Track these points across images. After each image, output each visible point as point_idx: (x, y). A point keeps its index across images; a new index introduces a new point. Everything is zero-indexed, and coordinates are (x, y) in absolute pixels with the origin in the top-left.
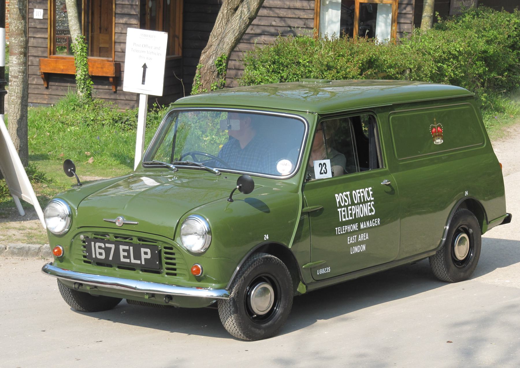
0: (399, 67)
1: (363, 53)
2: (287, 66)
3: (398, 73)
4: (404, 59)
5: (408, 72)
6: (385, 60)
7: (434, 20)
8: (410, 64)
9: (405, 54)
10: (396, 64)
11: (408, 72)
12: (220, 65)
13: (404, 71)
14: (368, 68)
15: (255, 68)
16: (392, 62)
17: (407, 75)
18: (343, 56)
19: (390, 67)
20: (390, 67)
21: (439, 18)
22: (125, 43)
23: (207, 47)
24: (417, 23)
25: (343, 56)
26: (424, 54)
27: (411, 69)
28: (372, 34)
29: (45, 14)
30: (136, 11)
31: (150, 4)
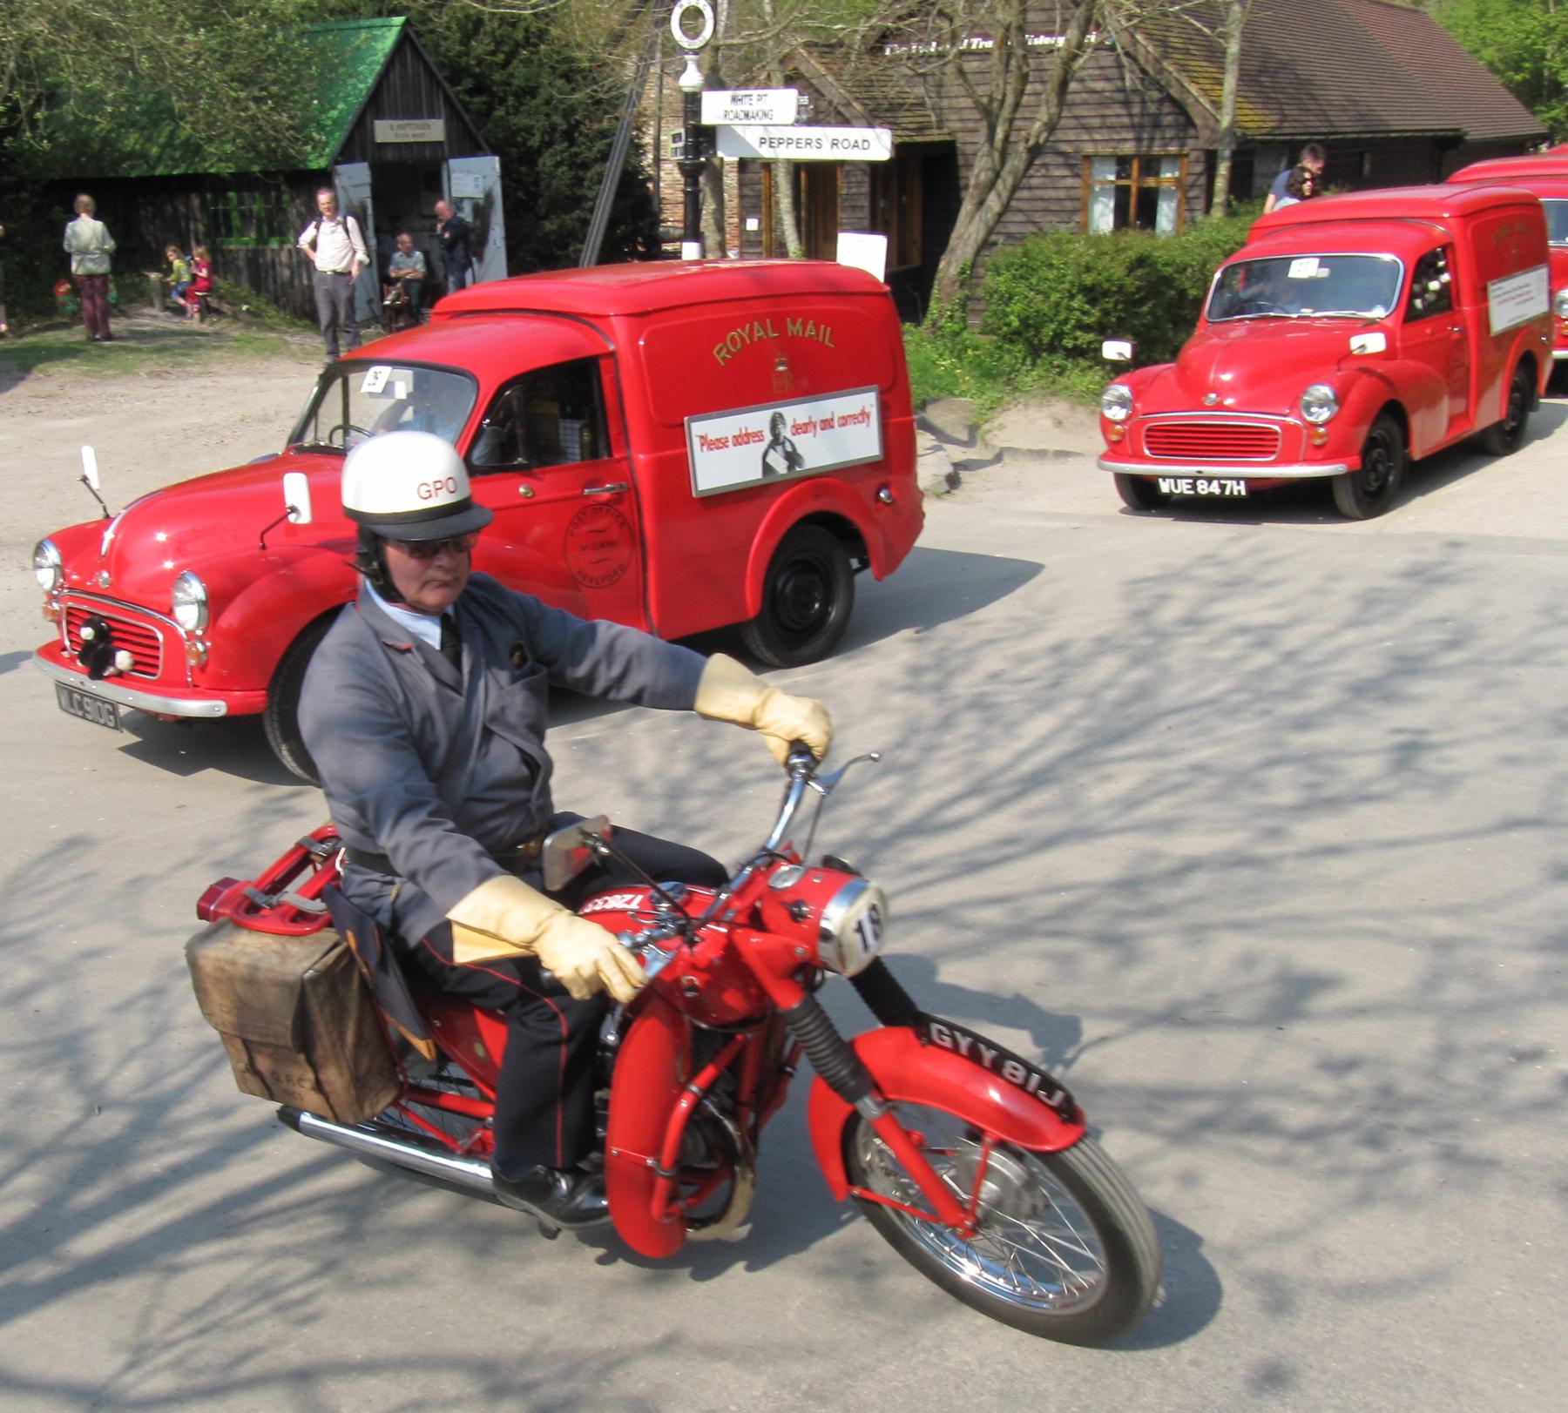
1: (1131, 248)
7: (1228, 205)
11: (1190, 270)
12: (963, 273)
13: (1184, 269)
15: (999, 274)
18: (1106, 254)
19: (1167, 265)
20: (1167, 265)
21: (1234, 203)
24: (1208, 209)
25: (1106, 254)
26: (1211, 247)
29: (760, 223)
30: (866, 213)
31: (882, 204)
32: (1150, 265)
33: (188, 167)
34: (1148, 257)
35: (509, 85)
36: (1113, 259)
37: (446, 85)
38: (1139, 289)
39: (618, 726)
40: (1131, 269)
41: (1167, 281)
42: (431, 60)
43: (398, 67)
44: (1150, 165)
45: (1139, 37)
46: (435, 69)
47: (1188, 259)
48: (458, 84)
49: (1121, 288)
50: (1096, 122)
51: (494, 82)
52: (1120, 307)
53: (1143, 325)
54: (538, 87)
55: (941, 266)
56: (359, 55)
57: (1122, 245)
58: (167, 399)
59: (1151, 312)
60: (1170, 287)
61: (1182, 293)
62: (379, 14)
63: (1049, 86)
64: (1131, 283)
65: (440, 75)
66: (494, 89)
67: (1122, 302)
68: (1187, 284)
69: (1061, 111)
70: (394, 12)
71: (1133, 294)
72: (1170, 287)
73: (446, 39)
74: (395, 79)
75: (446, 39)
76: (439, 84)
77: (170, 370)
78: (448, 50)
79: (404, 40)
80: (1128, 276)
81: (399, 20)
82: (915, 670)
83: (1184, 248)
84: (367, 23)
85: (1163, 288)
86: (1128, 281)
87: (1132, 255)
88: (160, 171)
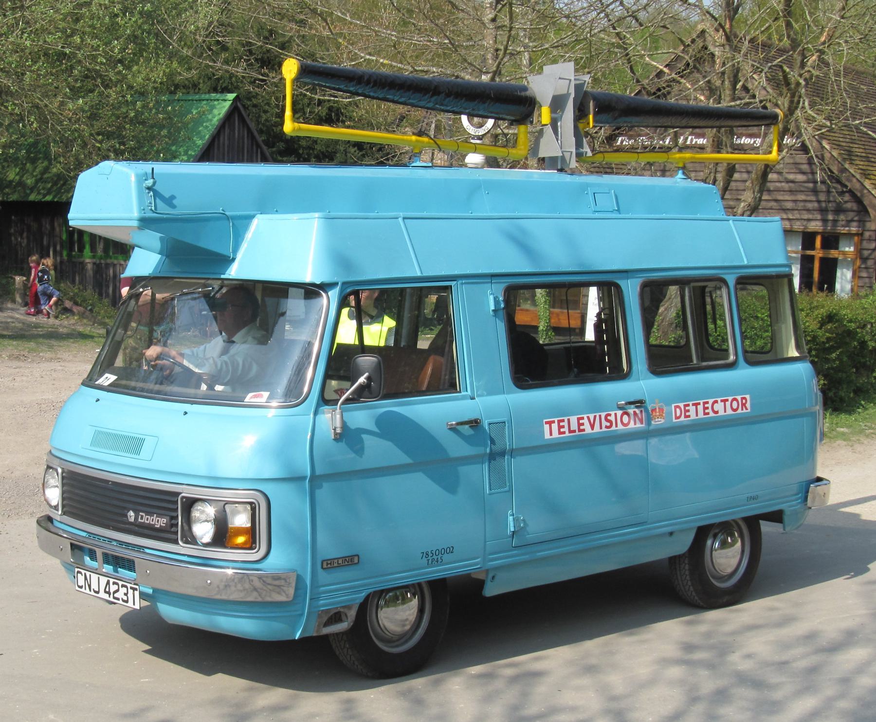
0: (860, 323)
1: (823, 307)
2: (745, 320)
3: (858, 328)
4: (865, 313)
5: (869, 326)
6: (845, 315)
8: (872, 318)
9: (865, 308)
10: (856, 318)
11: (869, 326)
13: (865, 326)
14: (829, 322)
16: (853, 316)
17: (867, 329)
19: (850, 321)
20: (850, 321)
22: (588, 296)
23: (666, 299)
27: (872, 324)
28: (831, 289)
32: (837, 321)
33: (55, 197)
34: (836, 314)
35: (313, 149)
36: (807, 315)
37: (265, 148)
38: (829, 339)
39: (437, 683)
40: (822, 324)
41: (850, 334)
42: (252, 125)
43: (227, 130)
44: (831, 241)
45: (825, 144)
46: (256, 134)
47: (868, 318)
48: (273, 147)
49: (814, 338)
50: (789, 205)
51: (300, 146)
52: (814, 353)
53: (833, 368)
54: (335, 153)
55: (660, 311)
56: (199, 120)
57: (815, 304)
58: (24, 378)
59: (838, 358)
60: (854, 339)
61: (863, 344)
62: (215, 90)
63: (753, 176)
64: (823, 335)
65: (260, 139)
66: (301, 151)
67: (815, 349)
68: (867, 338)
69: (762, 195)
70: (226, 90)
71: (823, 342)
72: (854, 339)
73: (266, 112)
74: (224, 139)
75: (266, 112)
76: (258, 146)
77: (26, 354)
78: (266, 120)
79: (234, 110)
80: (820, 328)
81: (231, 96)
82: (689, 648)
83: (864, 308)
84: (207, 96)
85: (848, 340)
86: (820, 333)
87: (823, 311)
88: (32, 197)
